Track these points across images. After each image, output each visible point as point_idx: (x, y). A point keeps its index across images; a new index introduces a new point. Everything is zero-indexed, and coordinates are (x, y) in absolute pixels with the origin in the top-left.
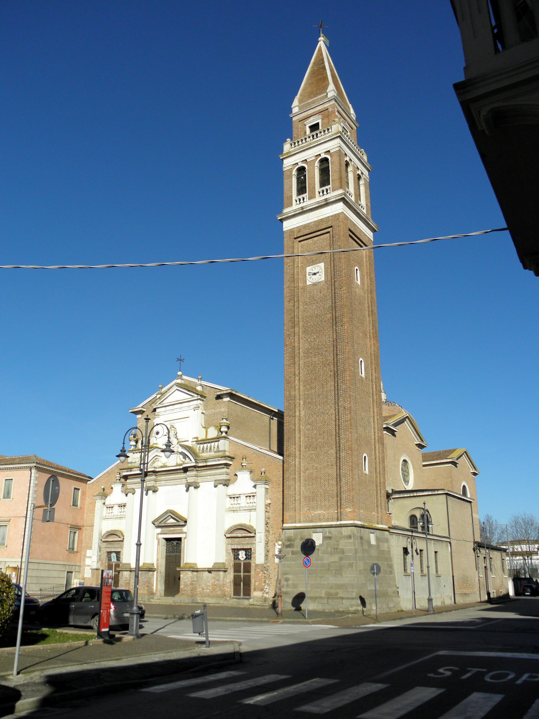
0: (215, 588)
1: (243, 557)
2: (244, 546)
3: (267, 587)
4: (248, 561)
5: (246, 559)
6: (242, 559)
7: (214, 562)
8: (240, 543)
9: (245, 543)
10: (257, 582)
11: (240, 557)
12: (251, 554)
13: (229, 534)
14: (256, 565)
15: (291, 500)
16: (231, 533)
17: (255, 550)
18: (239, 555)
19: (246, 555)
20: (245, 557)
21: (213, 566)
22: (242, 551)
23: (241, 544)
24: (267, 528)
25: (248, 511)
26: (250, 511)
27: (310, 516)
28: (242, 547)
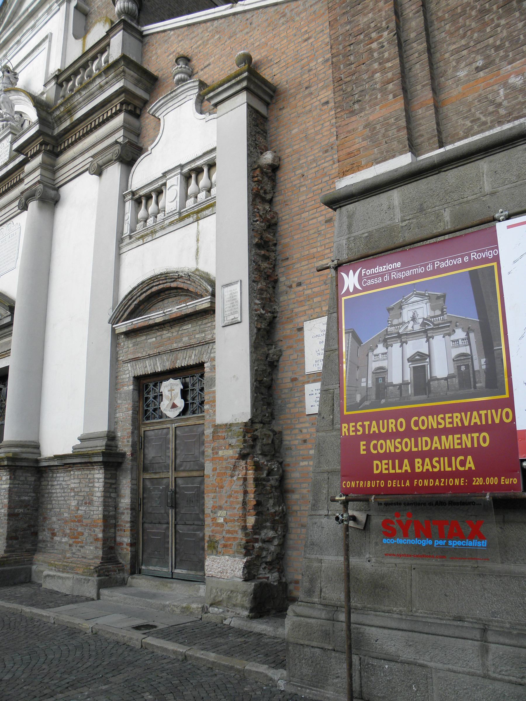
0: (80, 529)
1: (174, 406)
2: (177, 359)
3: (271, 534)
4: (191, 420)
5: (184, 412)
6: (172, 414)
7: (80, 432)
8: (162, 349)
9: (180, 345)
10: (220, 508)
11: (165, 406)
12: (202, 390)
13: (124, 321)
14: (217, 428)
15: (371, 51)
16: (132, 315)
17: (213, 368)
18: (159, 397)
19: (184, 394)
20: (180, 403)
21: (74, 448)
22: (171, 381)
23: (165, 353)
24: (264, 265)
25: (191, 220)
26: (197, 220)
27: (502, 92)
28: (168, 366)
